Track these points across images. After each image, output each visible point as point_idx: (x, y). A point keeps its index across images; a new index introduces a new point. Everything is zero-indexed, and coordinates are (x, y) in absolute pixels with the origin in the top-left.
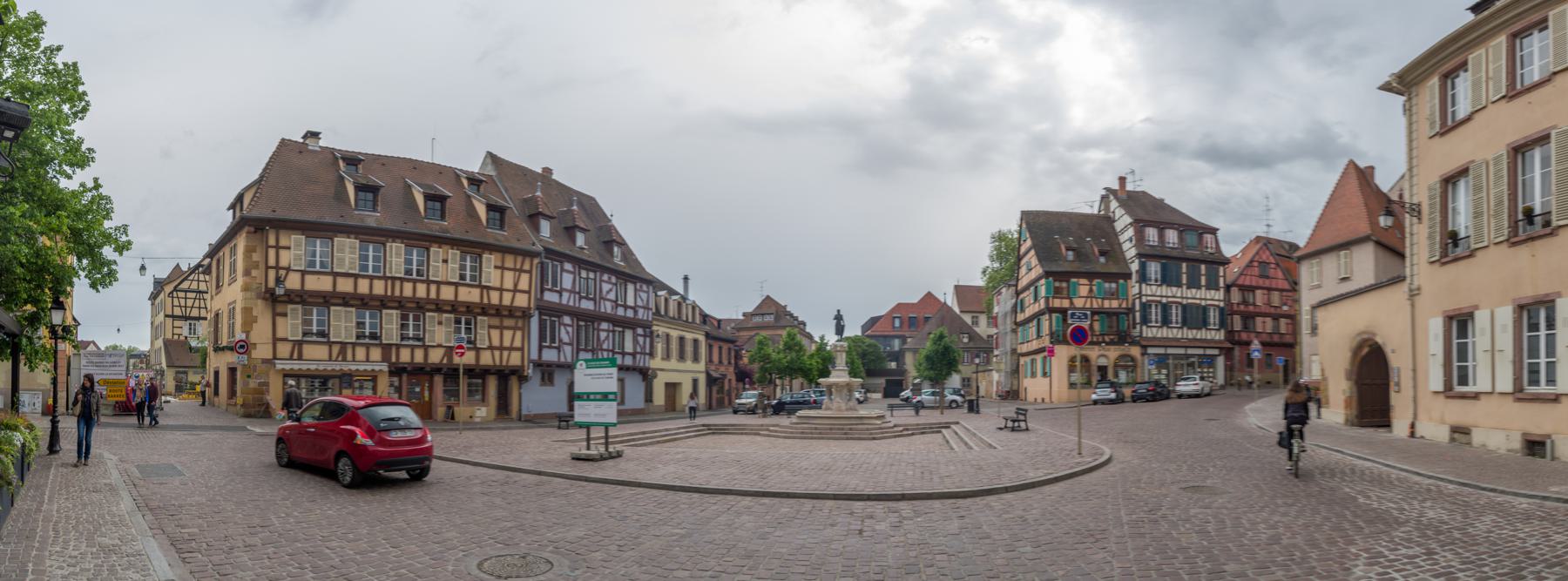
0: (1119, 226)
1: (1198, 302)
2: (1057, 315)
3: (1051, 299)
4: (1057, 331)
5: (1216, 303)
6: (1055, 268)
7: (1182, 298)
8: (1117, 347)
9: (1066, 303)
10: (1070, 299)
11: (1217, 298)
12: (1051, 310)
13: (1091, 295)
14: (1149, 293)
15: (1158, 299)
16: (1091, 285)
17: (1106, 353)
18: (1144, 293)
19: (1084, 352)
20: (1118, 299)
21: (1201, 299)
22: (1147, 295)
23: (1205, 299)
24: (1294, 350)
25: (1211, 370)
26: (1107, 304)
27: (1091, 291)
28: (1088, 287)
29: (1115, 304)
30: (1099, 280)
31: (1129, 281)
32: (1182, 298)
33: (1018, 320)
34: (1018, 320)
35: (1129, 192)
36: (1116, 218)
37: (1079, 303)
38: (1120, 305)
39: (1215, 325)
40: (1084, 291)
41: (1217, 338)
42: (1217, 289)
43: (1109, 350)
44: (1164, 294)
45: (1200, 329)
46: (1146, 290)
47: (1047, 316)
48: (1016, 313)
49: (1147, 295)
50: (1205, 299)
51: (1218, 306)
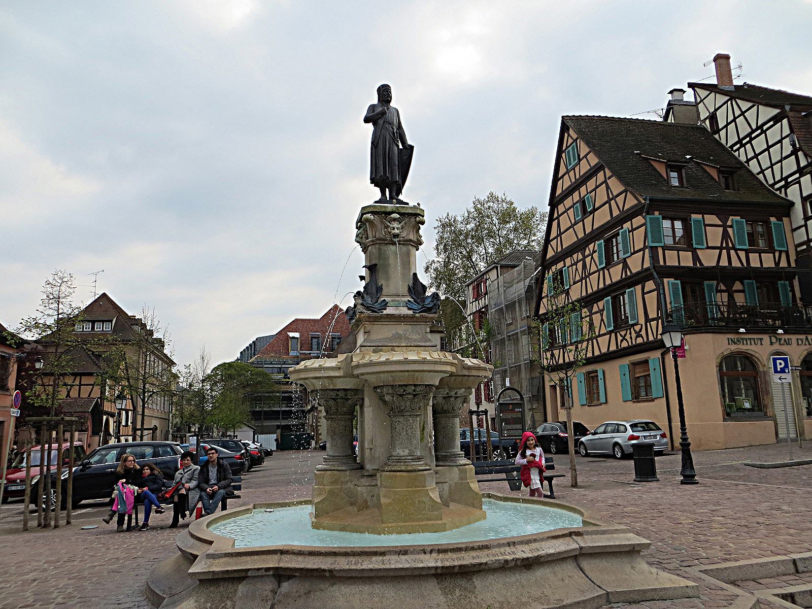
0: (727, 137)
2: (672, 280)
3: (660, 251)
4: (678, 310)
6: (660, 196)
8: (803, 337)
9: (687, 260)
12: (659, 272)
13: (726, 245)
16: (725, 227)
17: (785, 348)
19: (743, 347)
20: (771, 250)
26: (755, 262)
27: (725, 235)
29: (768, 261)
30: (738, 218)
31: (785, 219)
33: (542, 311)
35: (735, 86)
37: (709, 259)
38: (777, 264)
40: (714, 236)
43: (788, 343)
47: (650, 285)
48: (540, 298)
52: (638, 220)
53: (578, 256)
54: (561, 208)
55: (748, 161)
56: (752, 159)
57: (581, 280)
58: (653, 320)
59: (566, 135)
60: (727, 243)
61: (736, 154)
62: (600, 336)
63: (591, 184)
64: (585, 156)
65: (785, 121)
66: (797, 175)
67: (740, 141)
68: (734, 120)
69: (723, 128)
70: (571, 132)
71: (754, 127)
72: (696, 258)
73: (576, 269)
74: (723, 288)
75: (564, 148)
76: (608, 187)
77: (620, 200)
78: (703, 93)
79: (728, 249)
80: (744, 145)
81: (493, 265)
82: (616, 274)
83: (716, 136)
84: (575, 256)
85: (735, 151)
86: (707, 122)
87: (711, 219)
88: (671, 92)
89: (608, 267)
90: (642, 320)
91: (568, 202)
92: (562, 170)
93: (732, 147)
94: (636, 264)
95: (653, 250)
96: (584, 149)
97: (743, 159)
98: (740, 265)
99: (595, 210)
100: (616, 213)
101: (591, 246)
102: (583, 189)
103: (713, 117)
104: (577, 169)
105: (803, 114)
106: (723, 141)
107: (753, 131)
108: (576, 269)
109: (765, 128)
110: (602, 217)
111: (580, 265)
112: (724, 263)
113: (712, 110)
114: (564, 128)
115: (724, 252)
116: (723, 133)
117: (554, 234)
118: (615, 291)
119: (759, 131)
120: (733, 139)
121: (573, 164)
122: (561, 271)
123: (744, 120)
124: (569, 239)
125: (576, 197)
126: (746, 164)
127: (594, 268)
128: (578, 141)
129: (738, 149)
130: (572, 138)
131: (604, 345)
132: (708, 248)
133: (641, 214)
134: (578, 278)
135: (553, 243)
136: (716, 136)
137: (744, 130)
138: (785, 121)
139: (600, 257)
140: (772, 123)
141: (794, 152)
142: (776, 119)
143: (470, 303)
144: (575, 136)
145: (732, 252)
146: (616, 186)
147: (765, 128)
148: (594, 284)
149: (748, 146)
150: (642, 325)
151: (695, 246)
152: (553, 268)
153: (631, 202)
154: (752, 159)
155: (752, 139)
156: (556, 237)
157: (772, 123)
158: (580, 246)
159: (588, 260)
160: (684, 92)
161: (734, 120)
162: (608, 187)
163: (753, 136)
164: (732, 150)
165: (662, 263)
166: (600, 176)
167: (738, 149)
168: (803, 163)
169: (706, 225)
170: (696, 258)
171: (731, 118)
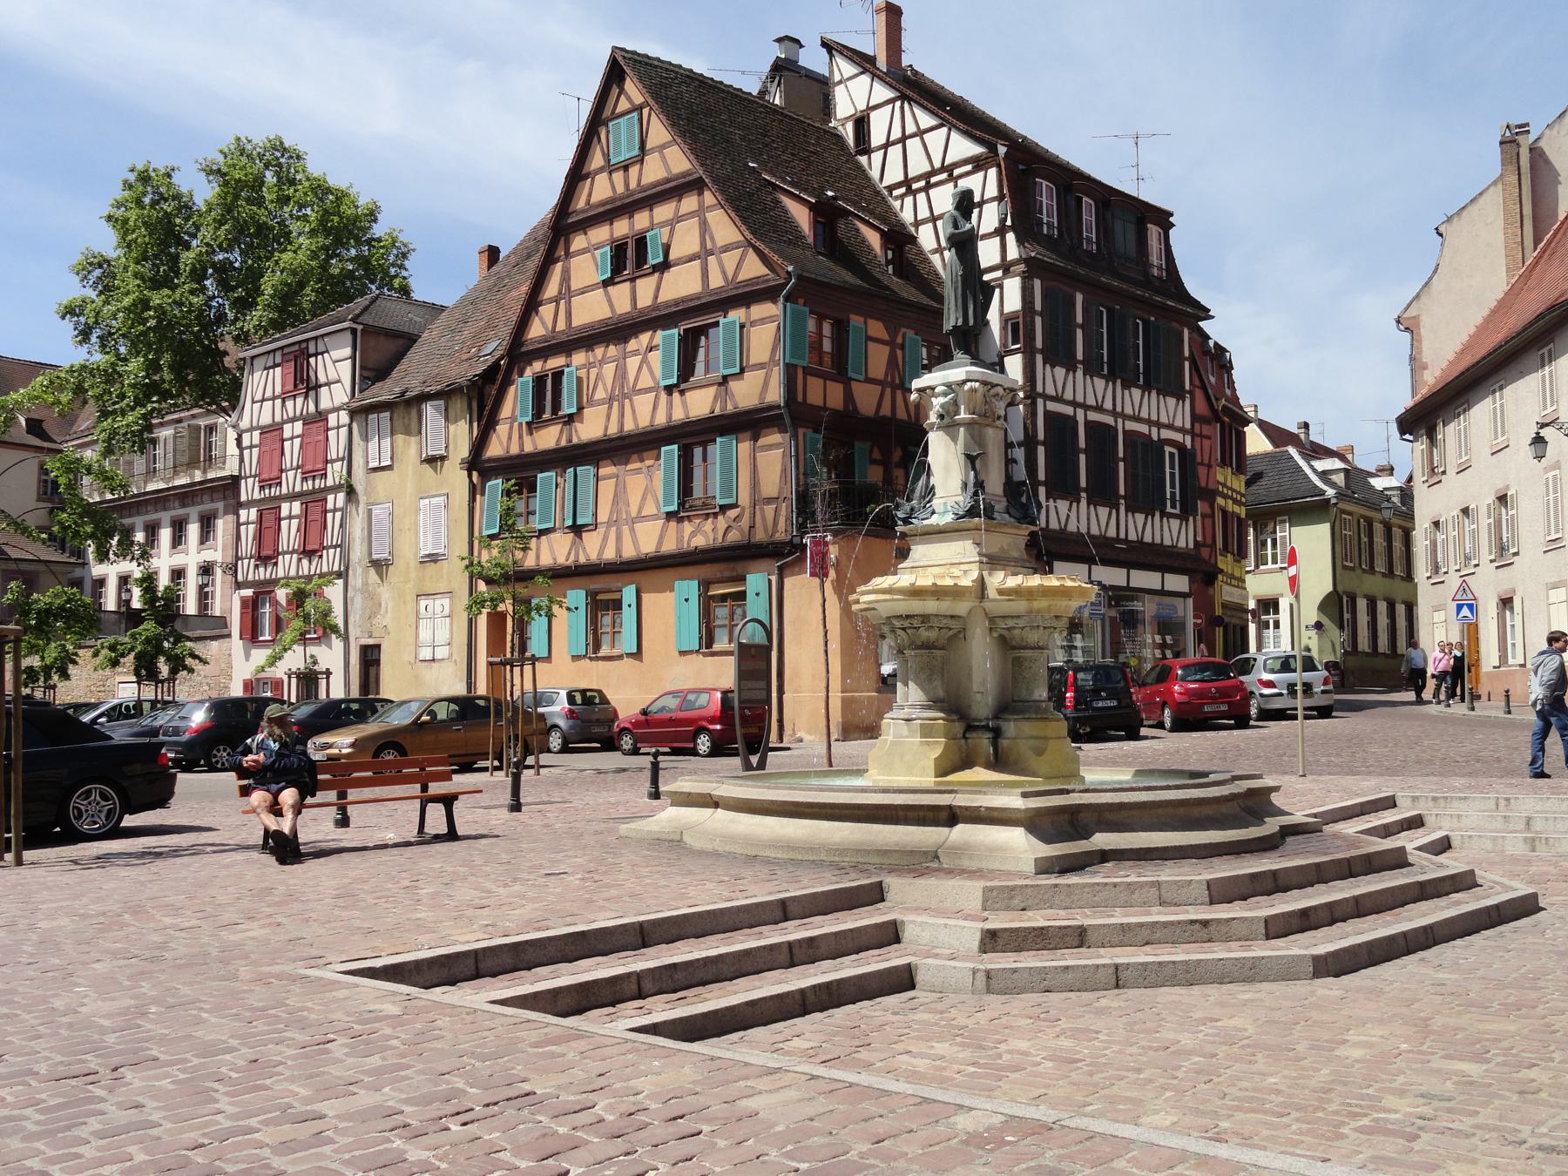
0: (886, 169)
1: (1144, 429)
5: (1178, 437)
7: (1114, 413)
9: (835, 396)
10: (847, 382)
11: (1178, 423)
14: (1050, 391)
15: (1069, 410)
18: (1039, 389)
21: (1149, 422)
22: (1047, 397)
23: (1159, 425)
24: (1211, 591)
25: (1169, 639)
28: (887, 349)
32: (1114, 413)
33: (495, 449)
34: (495, 449)
36: (877, 138)
39: (1174, 506)
41: (1182, 544)
42: (1180, 396)
44: (1080, 399)
45: (1149, 512)
46: (1052, 378)
49: (1047, 397)
50: (1159, 425)
51: (1181, 447)
52: (761, 310)
53: (612, 350)
54: (578, 242)
55: (917, 224)
56: (924, 221)
57: (610, 400)
58: (769, 500)
59: (615, 91)
60: (893, 378)
61: (897, 204)
62: (641, 518)
63: (664, 212)
64: (662, 147)
65: (992, 172)
66: (999, 274)
67: (907, 182)
68: (903, 140)
69: (879, 148)
70: (629, 86)
71: (937, 165)
72: (849, 396)
73: (598, 376)
74: (877, 455)
75: (607, 113)
76: (704, 227)
77: (731, 259)
78: (845, 68)
79: (894, 388)
80: (914, 193)
81: (346, 324)
82: (699, 403)
83: (863, 159)
84: (599, 351)
85: (896, 198)
86: (850, 126)
87: (877, 328)
88: (779, 40)
89: (683, 386)
90: (744, 499)
91: (600, 234)
92: (597, 160)
93: (891, 188)
94: (747, 393)
95: (790, 370)
96: (659, 132)
97: (907, 216)
98: (906, 418)
99: (665, 266)
100: (716, 281)
101: (645, 338)
102: (641, 220)
103: (862, 123)
104: (634, 171)
105: (1021, 167)
106: (875, 174)
107: (934, 172)
108: (598, 376)
109: (956, 172)
110: (682, 284)
111: (609, 370)
112: (886, 410)
113: (862, 106)
114: (615, 74)
115: (888, 391)
116: (877, 157)
117: (552, 289)
118: (692, 434)
119: (944, 176)
120: (894, 175)
121: (625, 155)
122: (558, 375)
123: (920, 145)
124: (591, 309)
125: (621, 228)
126: (913, 229)
127: (646, 381)
128: (646, 111)
129: (902, 197)
130: (629, 99)
131: (649, 539)
132: (869, 380)
133: (775, 301)
134: (600, 394)
135: (546, 311)
136: (863, 159)
137: (918, 166)
138: (992, 173)
139: (666, 363)
140: (969, 168)
141: (1000, 232)
142: (978, 164)
143: (253, 402)
144: (638, 99)
145: (899, 393)
146: (725, 228)
147: (956, 172)
148: (645, 413)
149: (921, 197)
150: (743, 509)
151: (851, 374)
152: (537, 366)
153: (754, 268)
154: (924, 221)
155: (929, 186)
156: (556, 300)
157: (969, 168)
158: (618, 332)
159: (633, 363)
160: (801, 46)
161: (903, 140)
162: (704, 227)
163: (933, 180)
164: (891, 194)
165: (800, 399)
166: (690, 203)
167: (902, 197)
168: (1013, 252)
169: (869, 338)
170: (849, 396)
171: (896, 134)
